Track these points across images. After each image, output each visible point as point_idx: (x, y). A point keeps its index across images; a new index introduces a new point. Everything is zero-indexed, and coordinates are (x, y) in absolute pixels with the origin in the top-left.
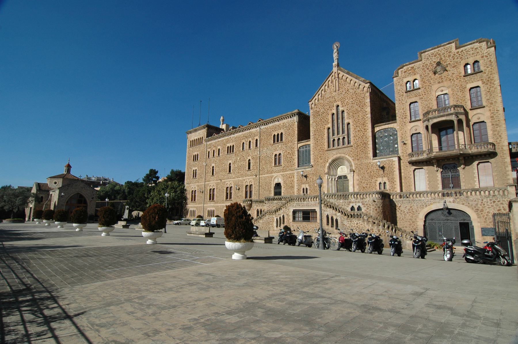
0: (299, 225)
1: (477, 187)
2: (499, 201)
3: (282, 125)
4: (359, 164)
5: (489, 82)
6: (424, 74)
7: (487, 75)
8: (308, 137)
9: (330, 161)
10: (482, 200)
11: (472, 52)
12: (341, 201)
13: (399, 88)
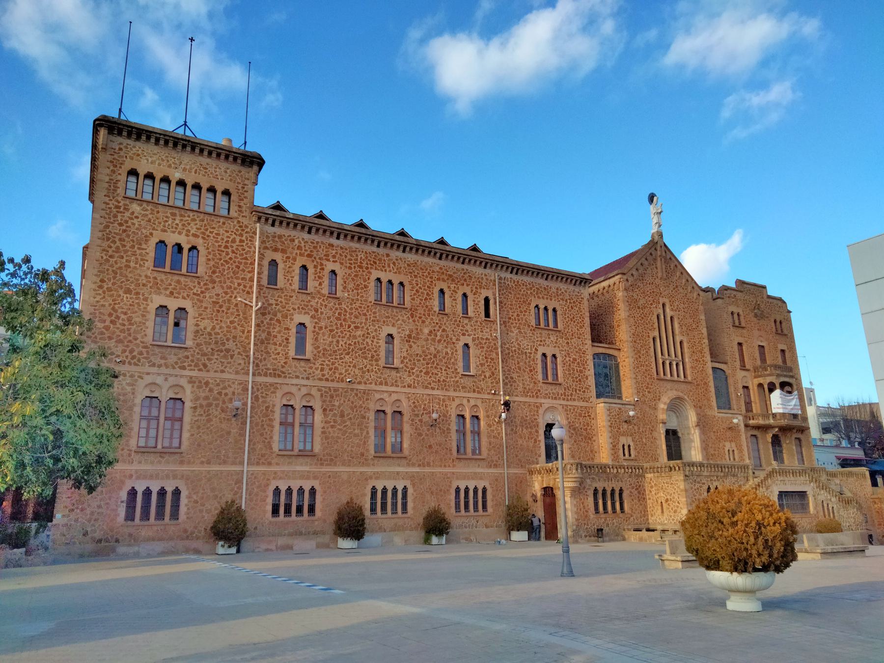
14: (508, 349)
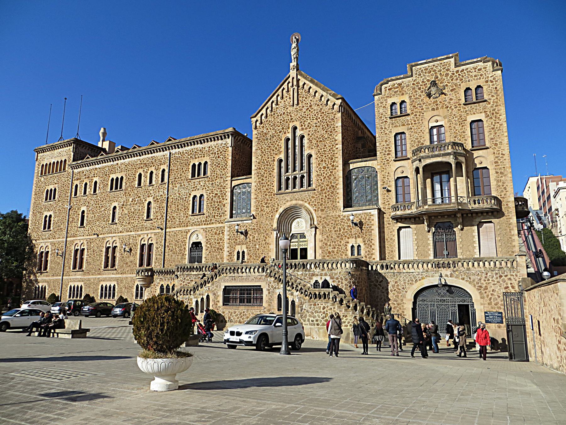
0: (232, 311)
1: (477, 256)
2: (506, 276)
3: (207, 149)
4: (323, 216)
5: (493, 115)
6: (414, 96)
7: (492, 107)
8: (248, 172)
9: (281, 210)
10: (487, 274)
11: (474, 73)
12: (300, 273)
13: (381, 111)
14: (172, 198)
